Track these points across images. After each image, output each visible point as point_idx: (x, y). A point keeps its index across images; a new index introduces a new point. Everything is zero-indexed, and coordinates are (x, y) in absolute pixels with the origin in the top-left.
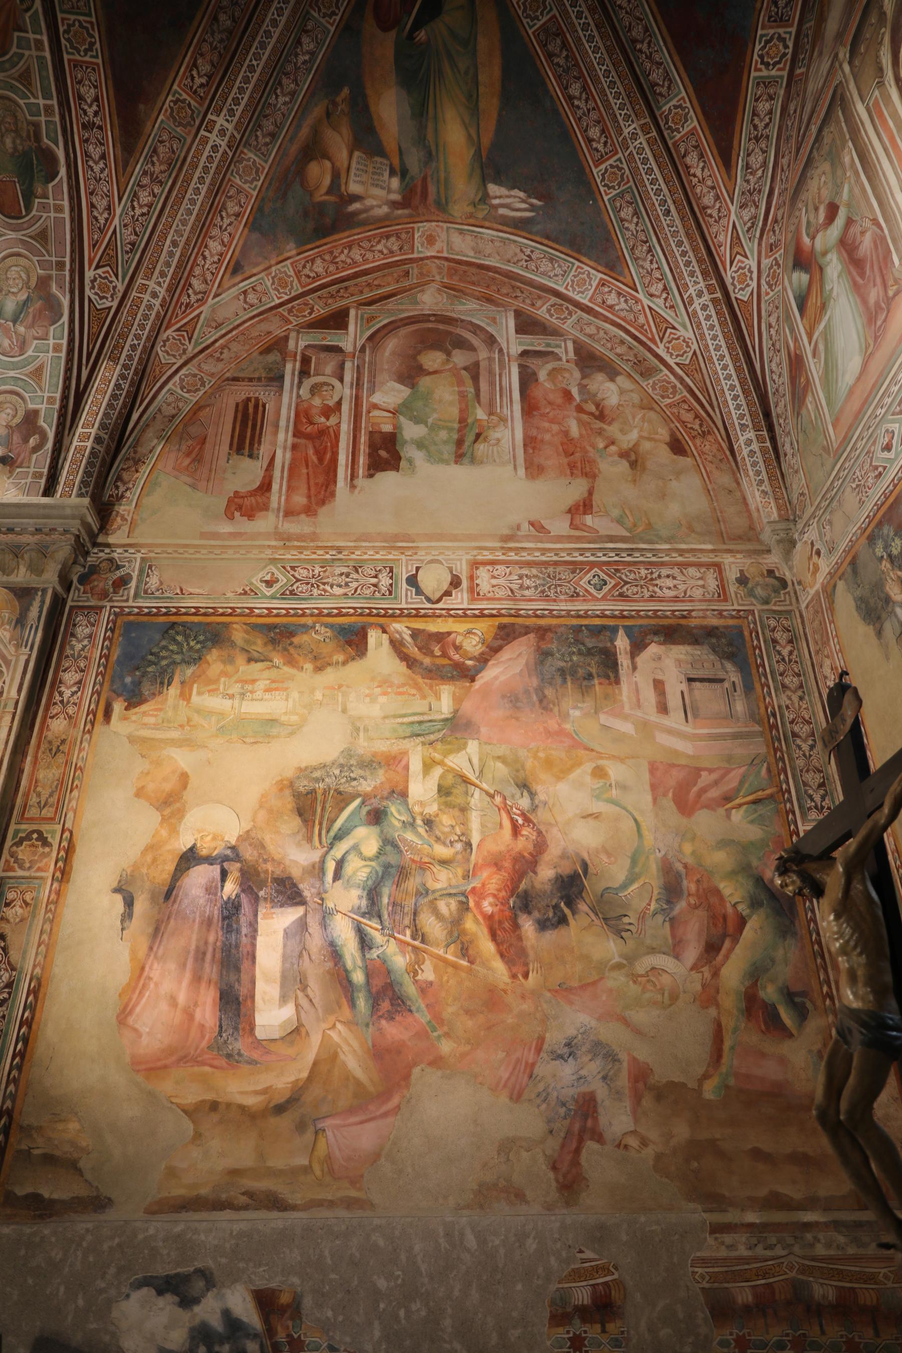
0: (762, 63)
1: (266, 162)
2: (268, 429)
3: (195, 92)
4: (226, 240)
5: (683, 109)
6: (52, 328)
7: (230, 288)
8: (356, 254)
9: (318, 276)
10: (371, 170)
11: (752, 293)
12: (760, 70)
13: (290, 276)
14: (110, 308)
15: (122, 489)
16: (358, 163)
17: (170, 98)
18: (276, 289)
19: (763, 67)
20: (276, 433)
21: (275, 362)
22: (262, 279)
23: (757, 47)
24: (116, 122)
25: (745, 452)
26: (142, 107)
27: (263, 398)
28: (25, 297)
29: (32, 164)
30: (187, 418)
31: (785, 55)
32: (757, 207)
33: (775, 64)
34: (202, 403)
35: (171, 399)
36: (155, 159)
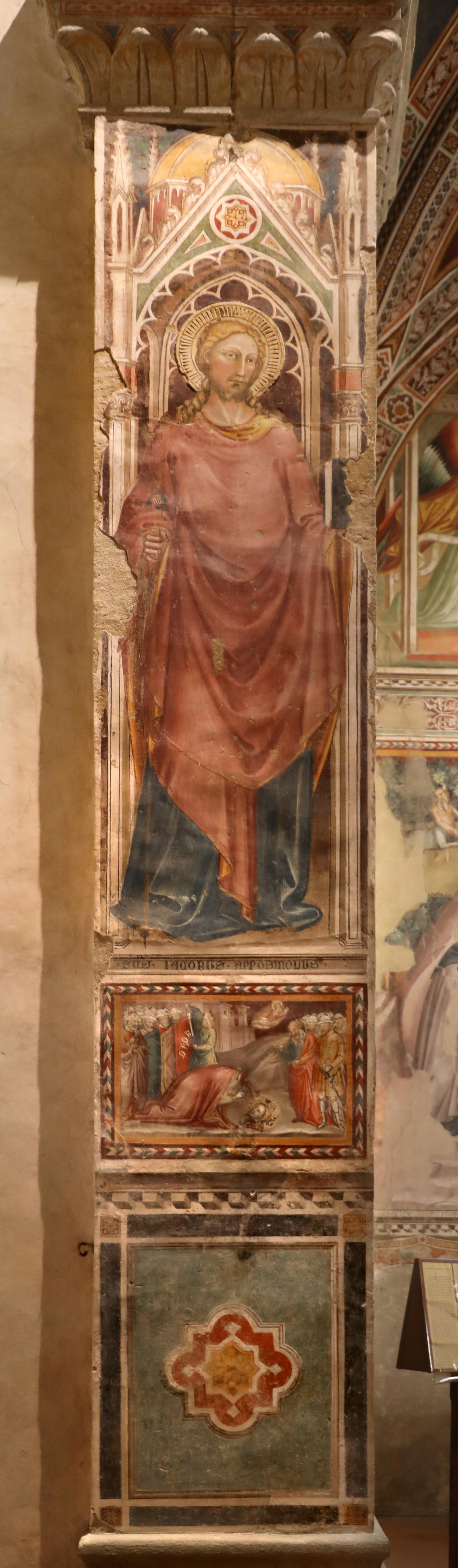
32: (426, 330)
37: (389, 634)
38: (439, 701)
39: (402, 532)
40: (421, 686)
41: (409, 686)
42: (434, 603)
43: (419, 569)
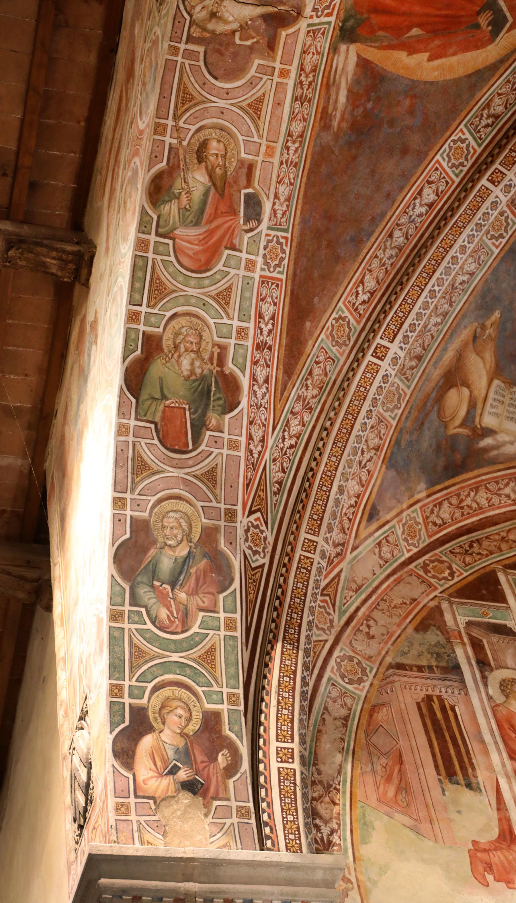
1: (409, 387)
2: (474, 747)
3: (357, 309)
4: (364, 478)
6: (221, 596)
7: (366, 539)
8: (482, 497)
9: (444, 524)
10: (507, 401)
13: (418, 524)
14: (262, 566)
15: (325, 831)
16: (496, 392)
17: (334, 315)
18: (406, 540)
20: (486, 752)
21: (438, 644)
22: (394, 527)
24: (284, 341)
26: (308, 324)
27: (449, 699)
28: (185, 553)
29: (209, 391)
30: (364, 721)
34: (373, 701)
35: (335, 693)
36: (309, 382)
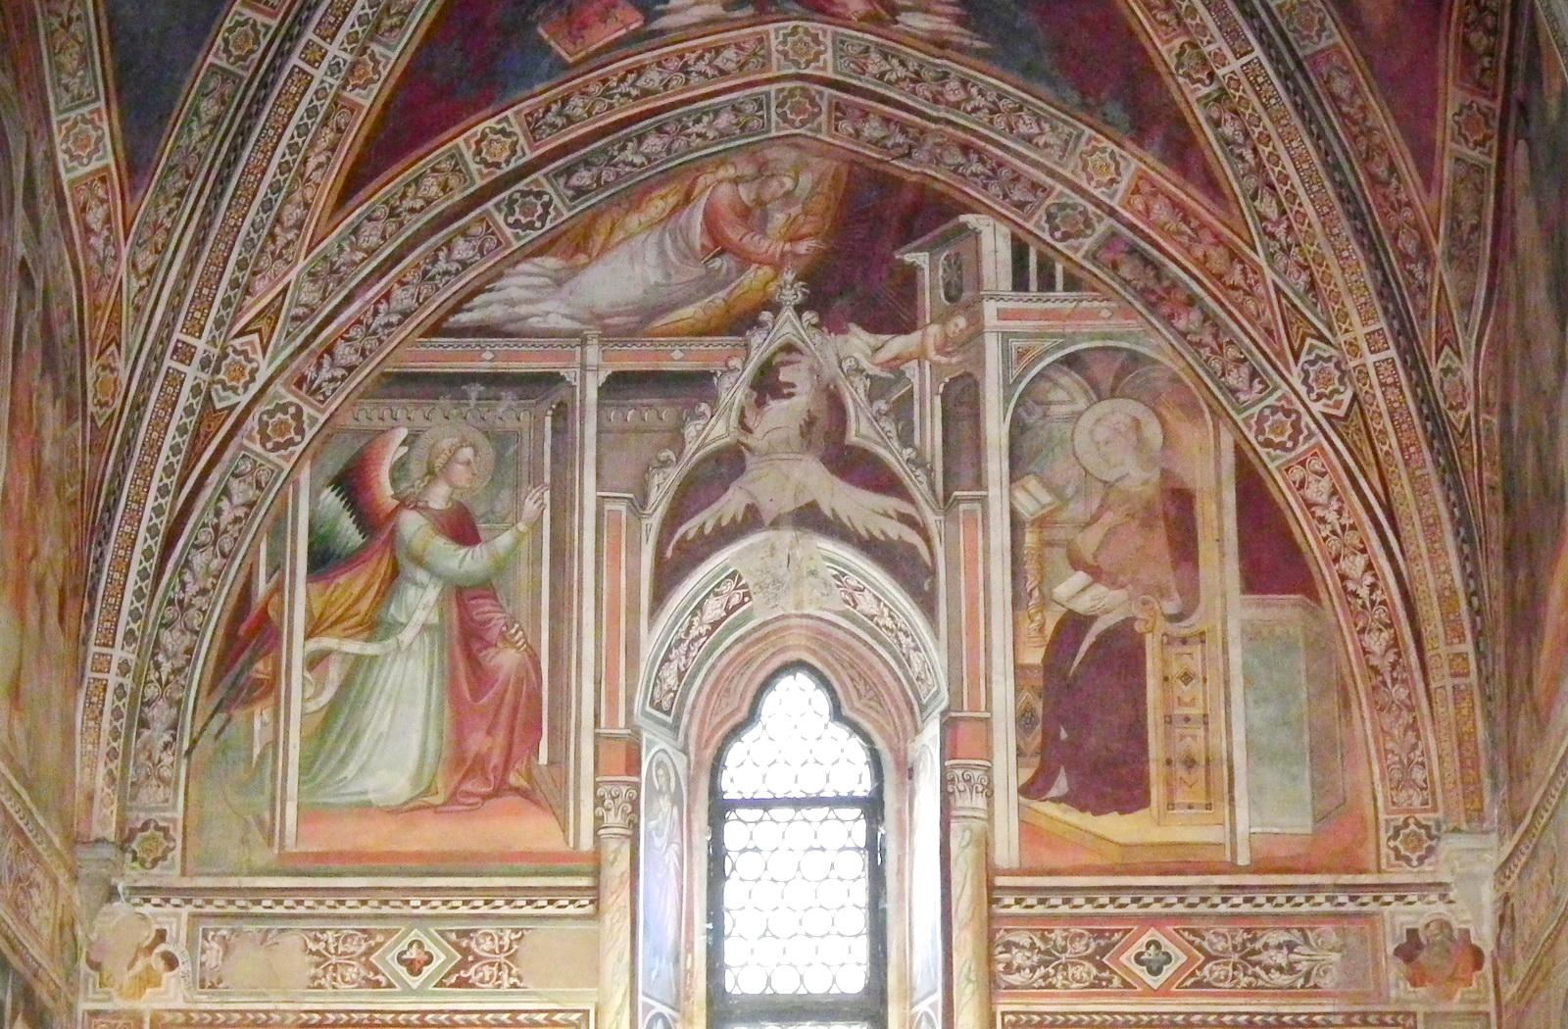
0: (478, 143)
5: (376, 70)
11: (232, 408)
12: (469, 148)
19: (474, 147)
23: (491, 123)
25: (113, 679)
31: (497, 165)
32: (323, 299)
33: (484, 162)
37: (250, 818)
38: (330, 936)
39: (278, 636)
40: (301, 910)
41: (279, 910)
42: (329, 758)
43: (304, 700)
